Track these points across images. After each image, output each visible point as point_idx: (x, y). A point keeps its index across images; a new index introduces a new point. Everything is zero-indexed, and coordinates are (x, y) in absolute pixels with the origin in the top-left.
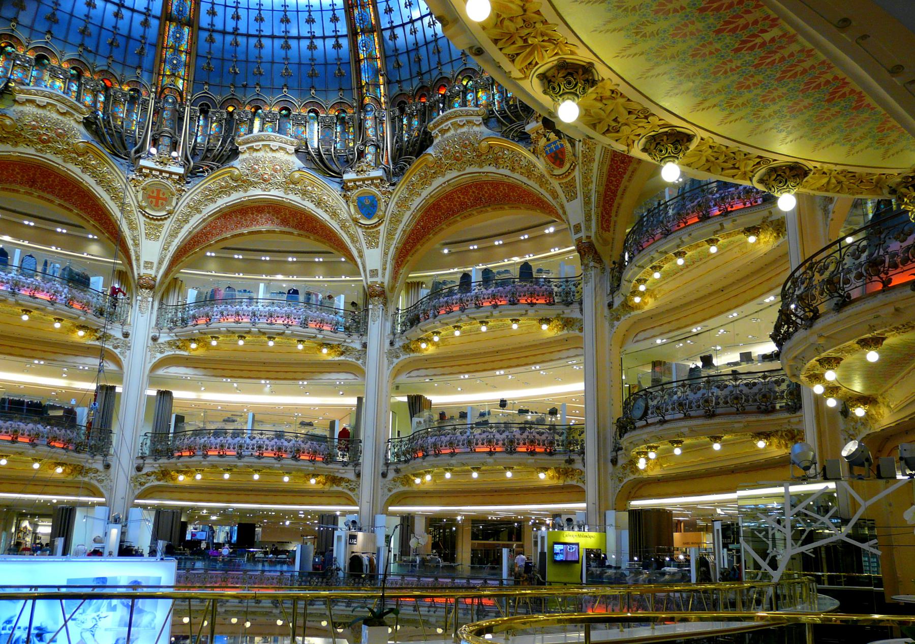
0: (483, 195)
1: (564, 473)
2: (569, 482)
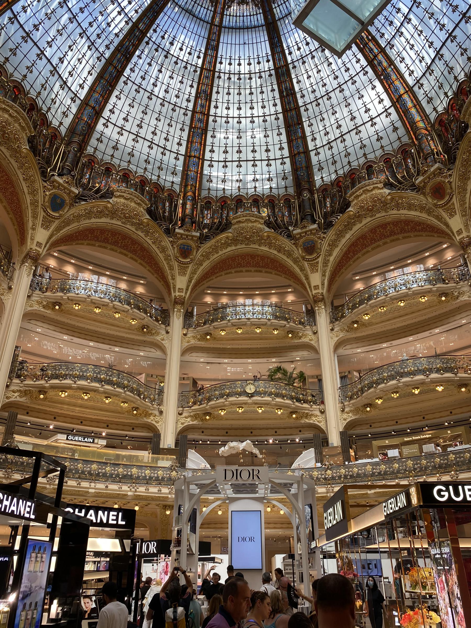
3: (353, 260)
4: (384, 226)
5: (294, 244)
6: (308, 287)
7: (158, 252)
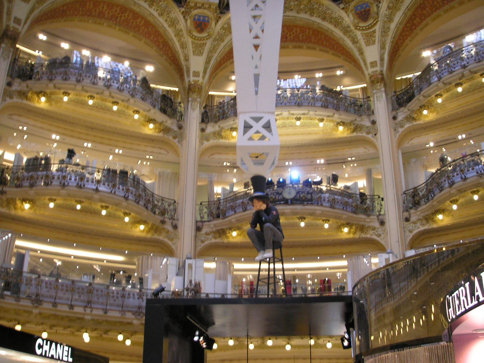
0: (121, 17)
1: (154, 229)
2: (156, 236)
3: (420, 27)
5: (343, 9)
6: (362, 64)
7: (166, 25)
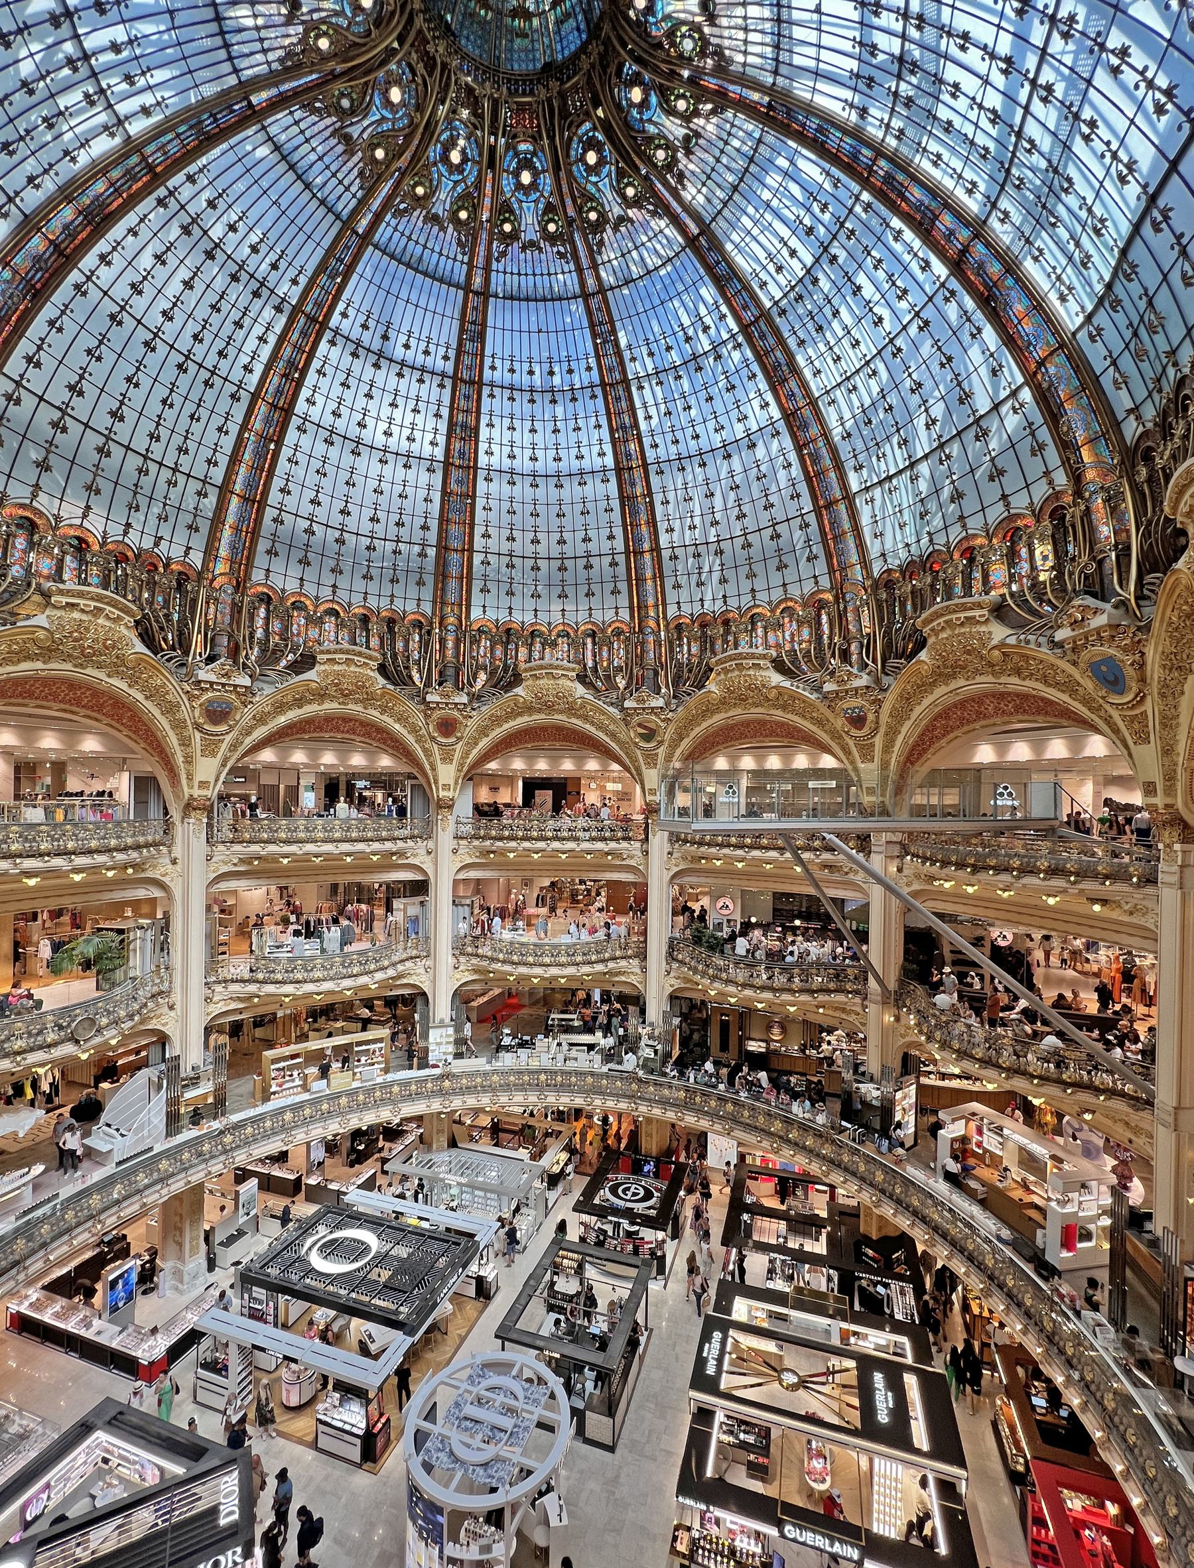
4: (346, 719)
6: (183, 777)
